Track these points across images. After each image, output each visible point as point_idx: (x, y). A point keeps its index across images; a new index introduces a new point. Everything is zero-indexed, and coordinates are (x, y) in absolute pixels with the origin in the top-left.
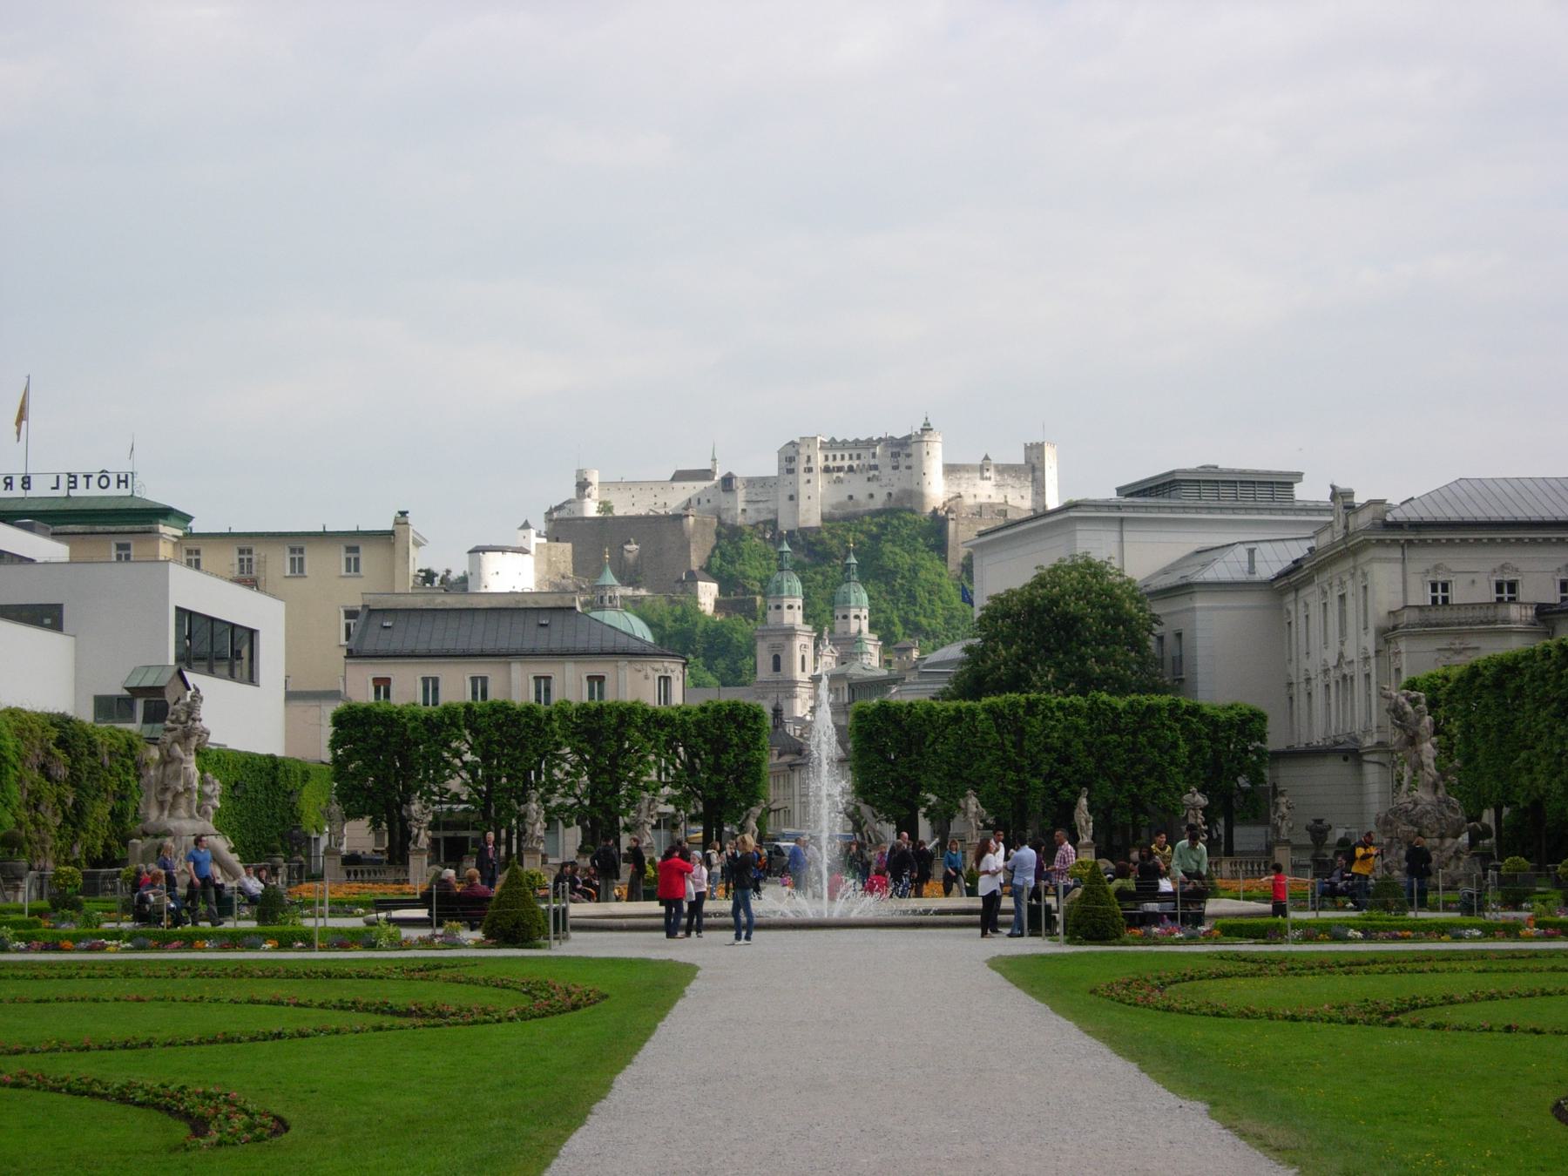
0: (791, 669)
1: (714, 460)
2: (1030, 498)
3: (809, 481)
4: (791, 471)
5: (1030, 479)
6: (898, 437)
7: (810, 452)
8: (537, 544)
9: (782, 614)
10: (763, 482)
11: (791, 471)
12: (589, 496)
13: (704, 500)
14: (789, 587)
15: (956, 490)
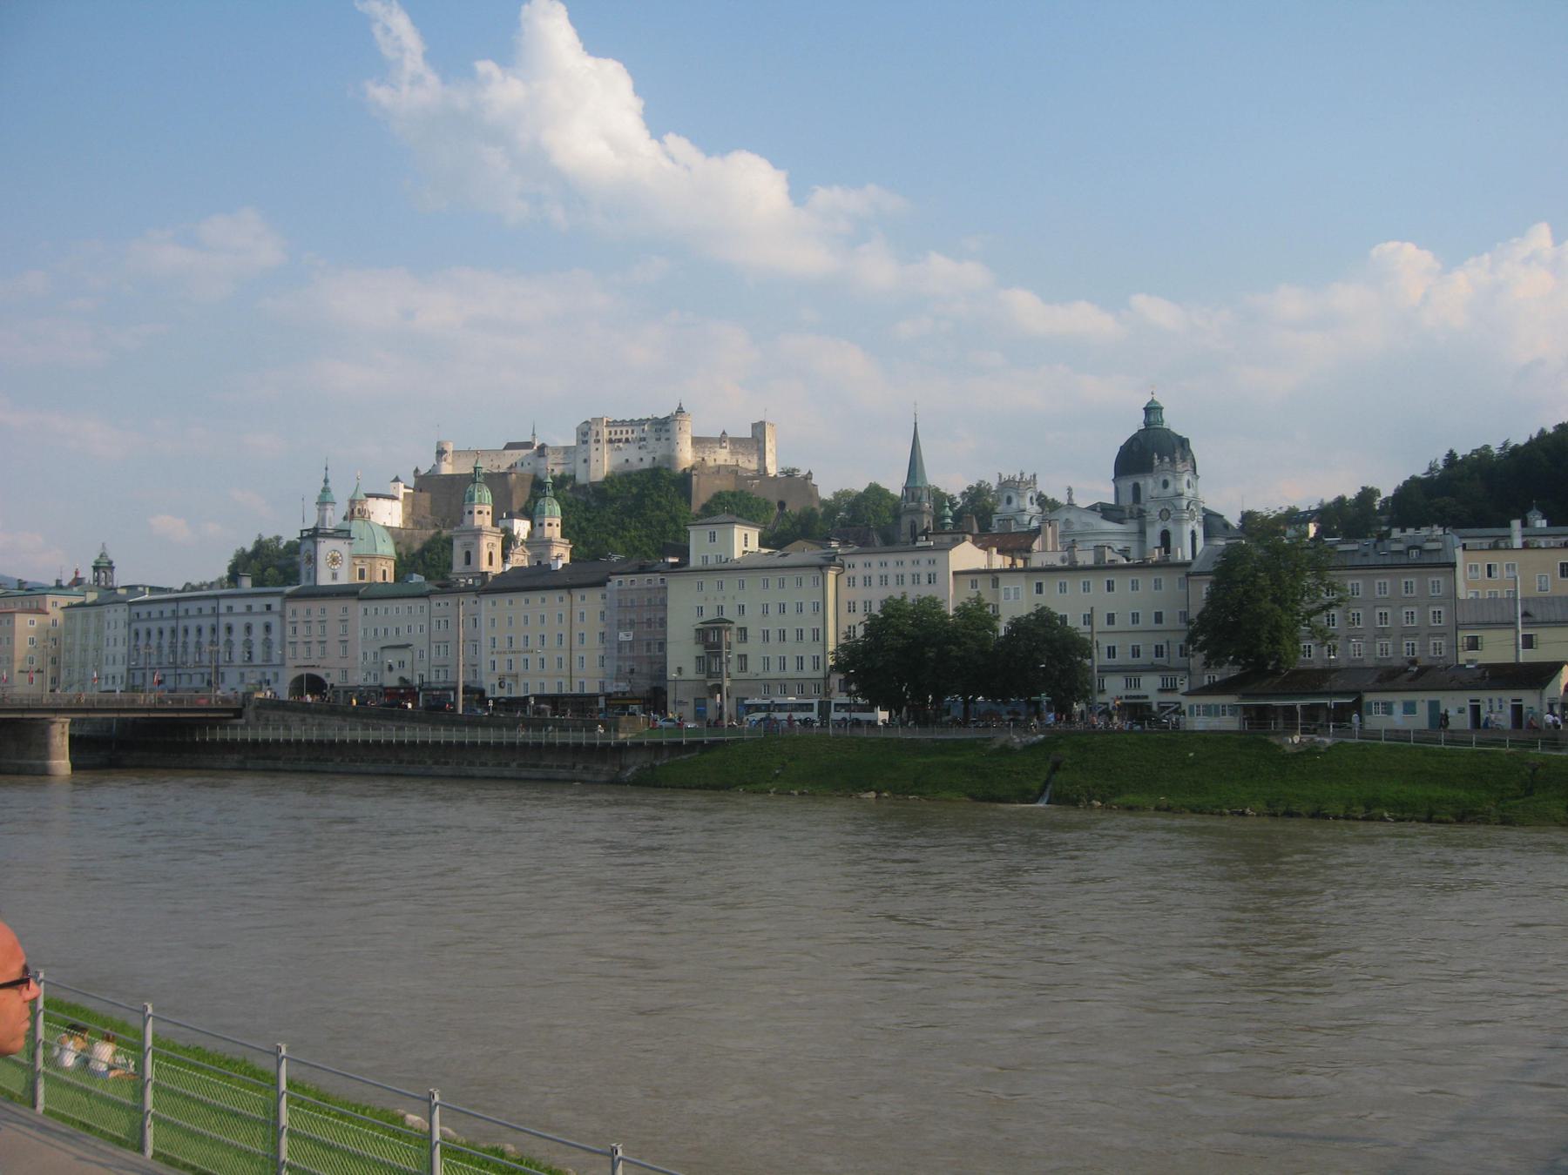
0: (478, 562)
1: (534, 435)
2: (756, 461)
3: (597, 449)
4: (585, 442)
5: (756, 448)
6: (661, 417)
7: (599, 428)
8: (405, 494)
9: (473, 517)
10: (567, 450)
11: (585, 442)
12: (445, 460)
13: (525, 464)
14: (480, 496)
15: (701, 455)
